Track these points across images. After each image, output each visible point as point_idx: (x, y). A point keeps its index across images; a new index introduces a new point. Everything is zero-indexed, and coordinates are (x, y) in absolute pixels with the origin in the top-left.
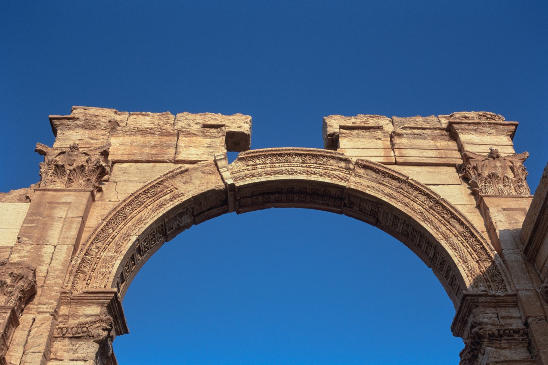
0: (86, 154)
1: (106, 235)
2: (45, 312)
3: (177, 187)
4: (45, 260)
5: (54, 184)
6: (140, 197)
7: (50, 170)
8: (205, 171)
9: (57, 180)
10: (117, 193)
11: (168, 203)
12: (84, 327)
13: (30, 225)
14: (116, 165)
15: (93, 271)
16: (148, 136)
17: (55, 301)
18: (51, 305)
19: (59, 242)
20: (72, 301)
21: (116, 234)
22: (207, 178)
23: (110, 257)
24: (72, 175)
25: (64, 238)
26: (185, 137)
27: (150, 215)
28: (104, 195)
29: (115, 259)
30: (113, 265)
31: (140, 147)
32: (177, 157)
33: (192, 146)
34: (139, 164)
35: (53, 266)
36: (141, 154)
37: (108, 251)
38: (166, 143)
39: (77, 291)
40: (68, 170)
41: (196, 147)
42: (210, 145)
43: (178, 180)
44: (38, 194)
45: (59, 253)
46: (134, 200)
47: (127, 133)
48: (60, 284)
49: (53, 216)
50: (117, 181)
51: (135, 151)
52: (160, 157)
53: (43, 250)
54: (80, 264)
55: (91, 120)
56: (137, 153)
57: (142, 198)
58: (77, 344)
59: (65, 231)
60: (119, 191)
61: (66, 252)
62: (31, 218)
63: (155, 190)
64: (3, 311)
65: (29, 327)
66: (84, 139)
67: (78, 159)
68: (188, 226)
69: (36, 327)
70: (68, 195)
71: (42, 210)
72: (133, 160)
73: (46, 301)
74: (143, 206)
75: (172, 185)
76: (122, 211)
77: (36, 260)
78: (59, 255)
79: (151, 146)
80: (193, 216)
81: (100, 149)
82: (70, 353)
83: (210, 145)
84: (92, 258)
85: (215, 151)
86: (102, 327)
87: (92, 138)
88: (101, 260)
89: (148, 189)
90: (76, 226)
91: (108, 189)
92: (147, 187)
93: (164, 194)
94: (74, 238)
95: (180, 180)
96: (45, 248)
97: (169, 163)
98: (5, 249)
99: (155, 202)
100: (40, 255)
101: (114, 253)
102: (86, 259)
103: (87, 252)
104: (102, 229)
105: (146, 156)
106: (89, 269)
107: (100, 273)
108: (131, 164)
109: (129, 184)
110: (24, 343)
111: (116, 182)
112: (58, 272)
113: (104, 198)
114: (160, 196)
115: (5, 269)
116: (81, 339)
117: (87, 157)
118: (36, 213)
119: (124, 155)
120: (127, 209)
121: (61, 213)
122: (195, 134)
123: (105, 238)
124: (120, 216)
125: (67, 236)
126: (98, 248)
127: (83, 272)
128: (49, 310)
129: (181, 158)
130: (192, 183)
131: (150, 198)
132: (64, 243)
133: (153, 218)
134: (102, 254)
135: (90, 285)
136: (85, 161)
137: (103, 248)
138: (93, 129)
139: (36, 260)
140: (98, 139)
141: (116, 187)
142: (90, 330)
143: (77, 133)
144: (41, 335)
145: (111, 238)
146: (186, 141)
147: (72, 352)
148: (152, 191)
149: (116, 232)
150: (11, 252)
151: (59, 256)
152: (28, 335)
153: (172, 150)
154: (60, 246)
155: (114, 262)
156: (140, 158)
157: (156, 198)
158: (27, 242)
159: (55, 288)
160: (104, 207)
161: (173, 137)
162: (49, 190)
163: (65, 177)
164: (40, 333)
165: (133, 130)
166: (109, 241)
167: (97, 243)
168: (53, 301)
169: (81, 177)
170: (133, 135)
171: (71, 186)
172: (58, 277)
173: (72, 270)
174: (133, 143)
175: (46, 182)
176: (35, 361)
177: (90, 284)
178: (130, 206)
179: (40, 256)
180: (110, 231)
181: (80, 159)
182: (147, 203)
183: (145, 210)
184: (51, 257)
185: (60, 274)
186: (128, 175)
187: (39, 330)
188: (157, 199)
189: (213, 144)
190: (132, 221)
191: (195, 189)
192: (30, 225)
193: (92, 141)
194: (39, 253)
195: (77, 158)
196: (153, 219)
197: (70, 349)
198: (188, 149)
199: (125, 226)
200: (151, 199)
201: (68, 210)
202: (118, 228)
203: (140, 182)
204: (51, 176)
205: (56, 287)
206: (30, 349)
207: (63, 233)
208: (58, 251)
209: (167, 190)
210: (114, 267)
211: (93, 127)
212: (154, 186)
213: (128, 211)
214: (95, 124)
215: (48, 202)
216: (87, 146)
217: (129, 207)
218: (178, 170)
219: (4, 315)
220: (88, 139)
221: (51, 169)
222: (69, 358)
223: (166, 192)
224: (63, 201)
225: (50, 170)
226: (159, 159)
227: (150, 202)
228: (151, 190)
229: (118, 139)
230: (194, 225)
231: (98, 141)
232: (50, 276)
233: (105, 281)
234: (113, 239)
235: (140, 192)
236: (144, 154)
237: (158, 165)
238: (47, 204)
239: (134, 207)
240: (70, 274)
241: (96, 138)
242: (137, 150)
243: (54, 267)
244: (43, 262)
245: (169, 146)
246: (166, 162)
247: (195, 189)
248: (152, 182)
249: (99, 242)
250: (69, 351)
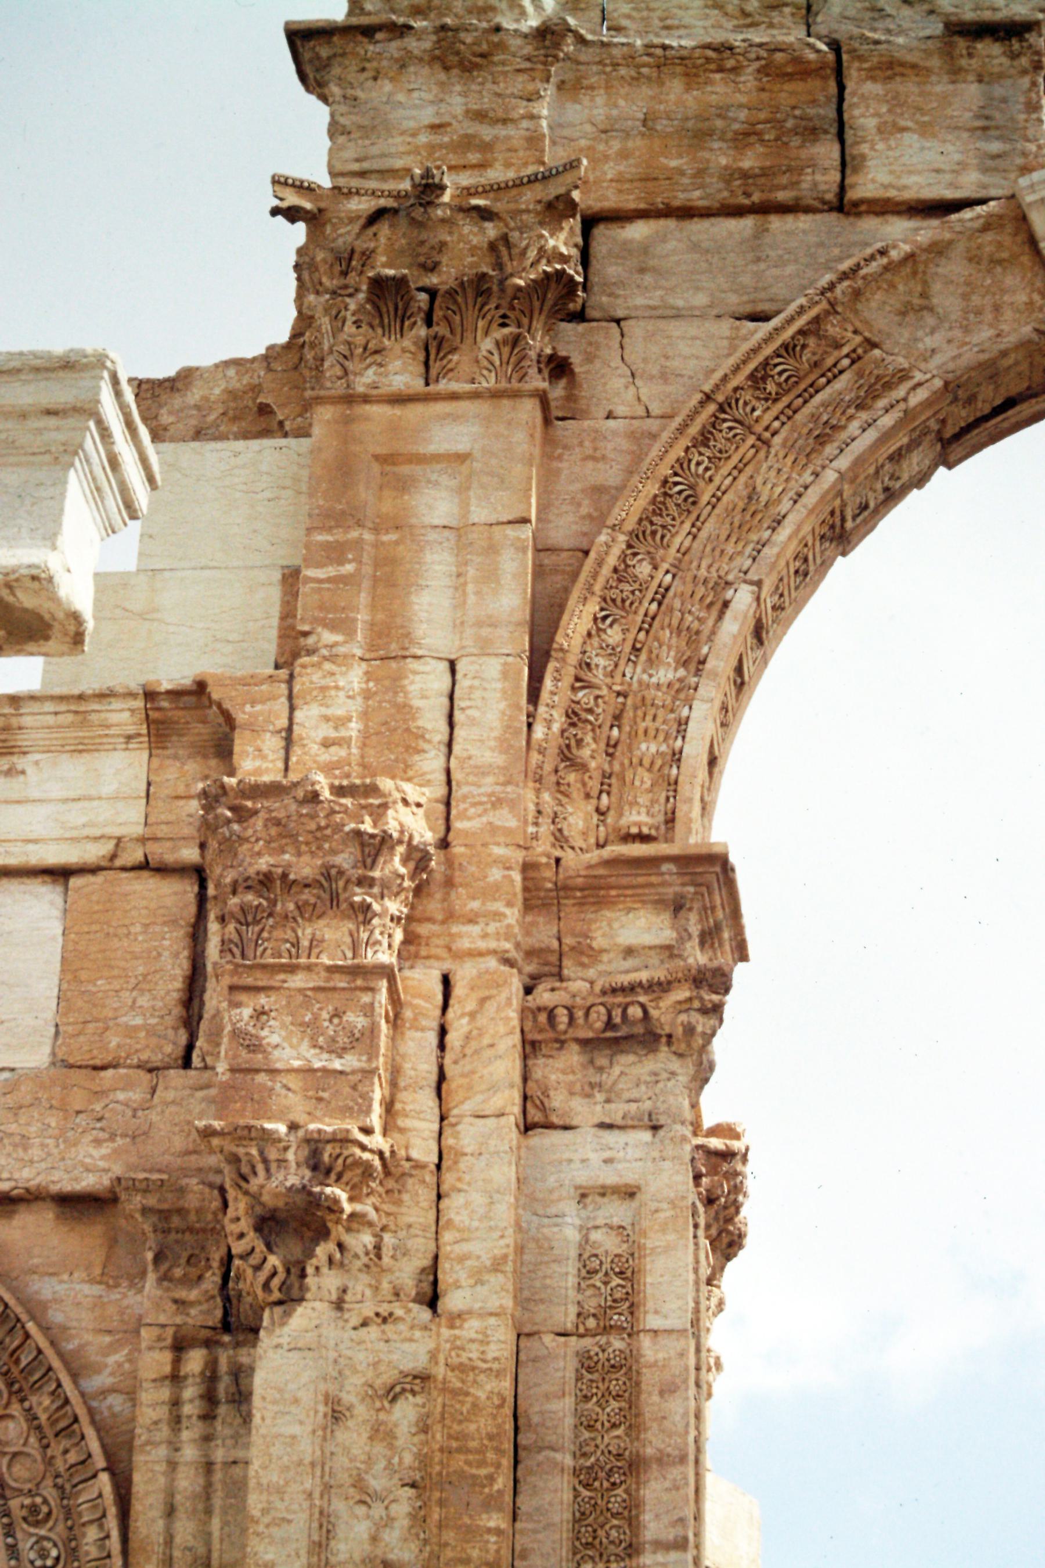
0: (485, 214)
1: (633, 592)
2: (481, 954)
3: (876, 339)
4: (429, 726)
5: (380, 365)
6: (737, 401)
7: (350, 295)
8: (979, 253)
9: (386, 342)
10: (633, 375)
11: (851, 418)
12: (632, 1003)
13: (331, 571)
14: (600, 232)
15: (611, 750)
16: (711, 82)
17: (510, 904)
18: (498, 924)
19: (465, 643)
20: (562, 893)
21: (669, 577)
22: (989, 281)
23: (664, 689)
24: (446, 318)
25: (479, 624)
26: (873, 79)
27: (787, 480)
28: (581, 386)
29: (682, 696)
31: (686, 141)
32: (852, 186)
33: (910, 124)
34: (698, 227)
35: (465, 754)
36: (700, 173)
37: (650, 660)
38: (797, 112)
39: (573, 848)
40: (420, 289)
41: (925, 130)
42: (987, 118)
43: (873, 304)
44: (328, 416)
45: (477, 694)
46: (715, 422)
47: (623, 71)
48: (508, 832)
49: (414, 521)
50: (620, 314)
51: (674, 163)
52: (785, 188)
53: (412, 682)
54: (563, 731)
55: (467, 30)
56: (682, 173)
57: (746, 404)
58: (611, 1063)
59: (478, 593)
60: (639, 366)
61: (504, 691)
62: (330, 538)
63: (791, 361)
64: (359, 982)
65: (438, 1012)
66: (449, 124)
67: (455, 238)
68: (920, 480)
69: (463, 1015)
70: (449, 415)
71: (363, 495)
72: (667, 205)
73: (475, 905)
74: (751, 440)
75: (855, 332)
76: (676, 474)
77: (395, 730)
78: (479, 703)
79: (736, 133)
80: (941, 440)
81: (538, 186)
82: (592, 1101)
83: (987, 118)
84: (597, 697)
85: (1008, 147)
86: (696, 1004)
87: (480, 116)
88: (630, 701)
89: (765, 364)
90: (515, 564)
91: (590, 359)
92: (760, 358)
93: (829, 374)
94: (519, 624)
95: (884, 303)
96: (415, 673)
97: (822, 211)
98: (264, 687)
99: (798, 417)
100: (405, 705)
101: (676, 670)
102: (577, 708)
103: (578, 679)
104: (615, 570)
105: (721, 185)
106: (594, 746)
107: (641, 764)
108: (662, 222)
109: (675, 328)
110: (434, 1077)
111: (618, 321)
112: (490, 779)
113: (583, 403)
114: (811, 385)
115: (327, 816)
116: (624, 1045)
117: (491, 230)
118: (343, 512)
119: (627, 186)
120: (694, 462)
122: (914, 66)
123: (632, 604)
124: (671, 496)
125: (490, 617)
126: (612, 652)
127: (583, 767)
128: (493, 944)
129: (871, 186)
130: (931, 309)
131: (775, 401)
132: (485, 649)
133: (800, 495)
134: (628, 675)
135: (612, 813)
136: (485, 245)
137: (628, 648)
138: (476, 66)
139: (395, 730)
140: (512, 120)
141: (622, 348)
142: (654, 1013)
143: (416, 94)
144: (492, 1046)
145: (653, 600)
146: (877, 98)
147: (600, 1097)
148: (779, 368)
149: (667, 572)
150: (290, 697)
151: (477, 707)
152: (442, 1046)
153: (827, 151)
154: (472, 663)
155: (685, 712)
156: (696, 197)
157: (799, 396)
158: (342, 650)
159: (498, 851)
160: (595, 449)
161: (818, 83)
162: (366, 399)
163: (415, 323)
164: (486, 1041)
165: (646, 59)
166: (646, 615)
167: (604, 631)
168: (499, 906)
169: (481, 324)
170: (649, 79)
171: (451, 370)
172: (497, 802)
173: (540, 767)
174: (654, 120)
175: (345, 357)
176: (492, 1149)
177: (608, 809)
178: (702, 449)
179: (405, 710)
180: (644, 569)
181: (462, 238)
182: (765, 423)
183: (762, 454)
184: (445, 710)
185: (498, 788)
186: (663, 283)
187: (479, 1024)
188: (800, 400)
189: (997, 115)
190: (716, 511)
191: (949, 341)
192: (331, 571)
193: (487, 132)
194: (400, 699)
195: (450, 233)
196: (804, 500)
197: (590, 1083)
198: (892, 143)
199: (695, 537)
200: (780, 405)
202: (673, 551)
203: (719, 317)
204: (357, 324)
205: (498, 844)
206: (462, 1102)
207: (472, 599)
208: (471, 687)
209: (836, 354)
210: (688, 735)
211: (478, 60)
212: (785, 346)
213: (701, 469)
214: (485, 47)
215: (377, 457)
216: (473, 157)
217: (701, 454)
218: (874, 264)
219: (366, 998)
220: (466, 123)
221: (351, 290)
222: (596, 1121)
223: (835, 365)
224: (432, 448)
225: (348, 300)
226: (782, 196)
227: (777, 418)
228: (776, 365)
229: (586, 100)
230: (942, 470)
231: (510, 131)
232: (465, 797)
233: (664, 795)
234: (660, 604)
235: (734, 383)
236: (712, 176)
237: (776, 223)
238: (376, 468)
239: (720, 452)
240: (537, 785)
241: (500, 114)
242: (680, 156)
243: (470, 758)
244: (423, 737)
245: (811, 132)
246: (808, 210)
247: (949, 341)
248: (776, 329)
249: (611, 625)
250: (587, 1088)
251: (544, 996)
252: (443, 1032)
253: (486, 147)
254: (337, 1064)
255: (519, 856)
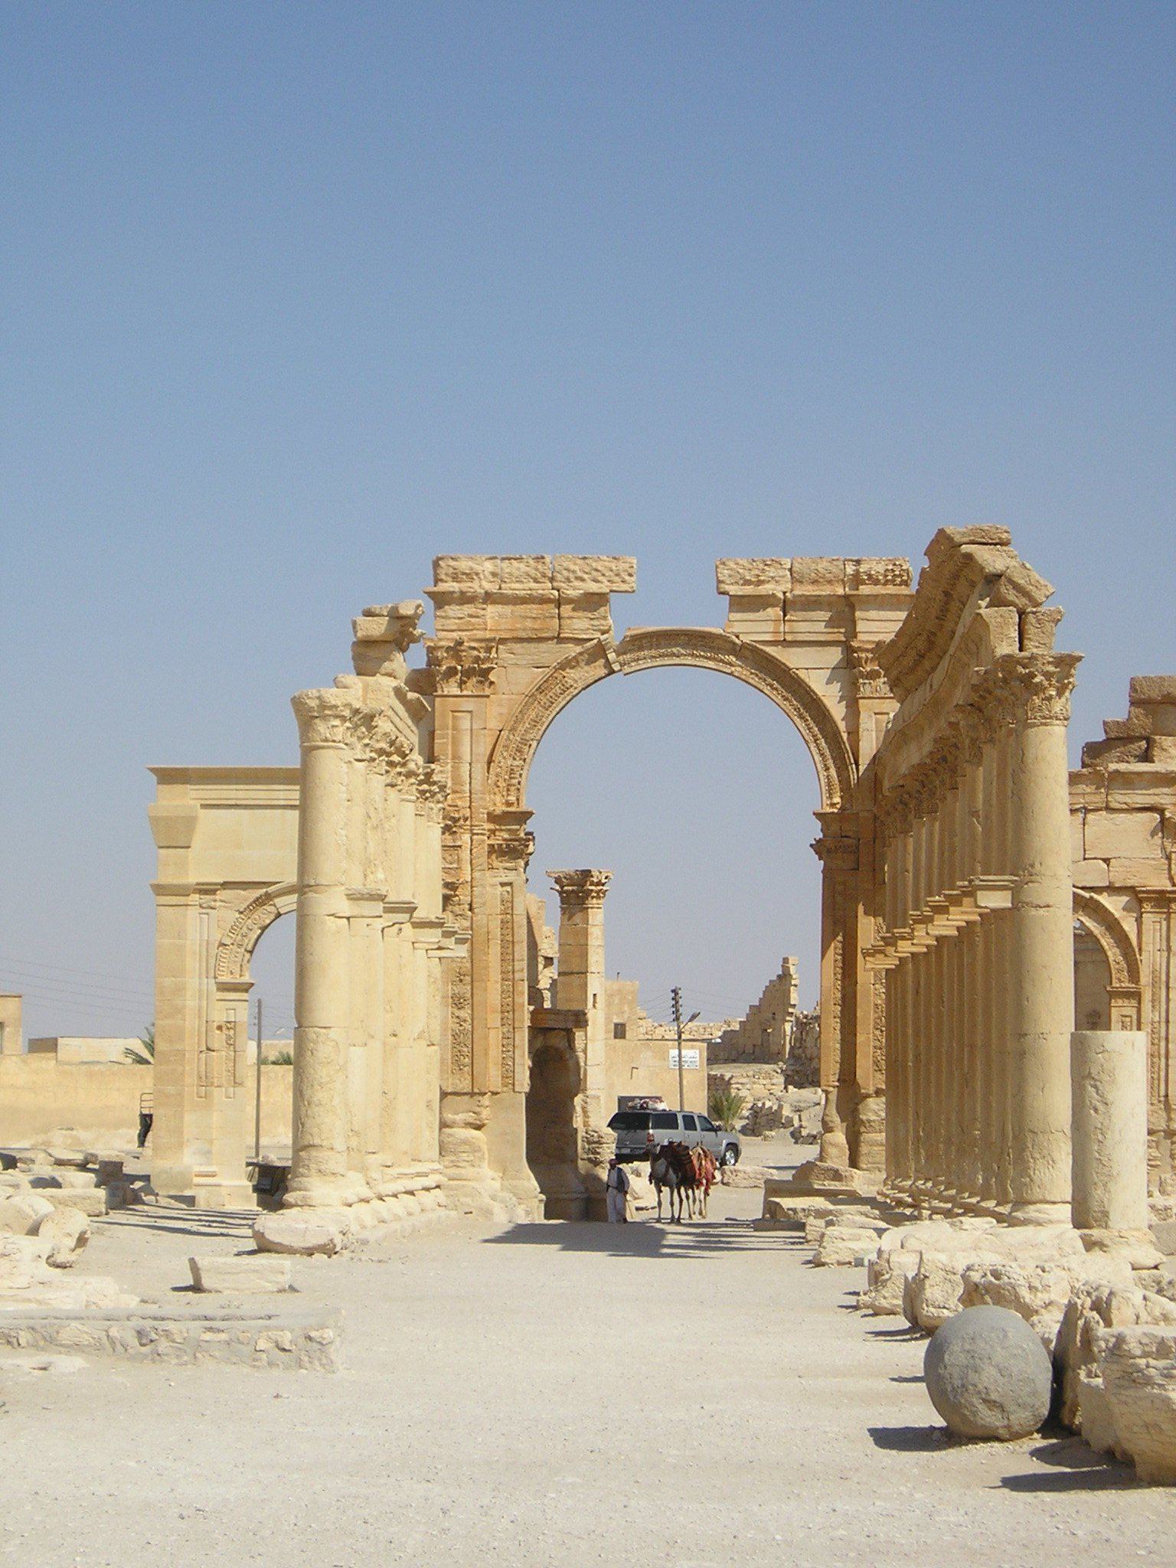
0: (474, 648)
30: (521, 775)
87: (470, 616)
117: (475, 653)
121: (465, 723)
152: (471, 854)
156: (524, 635)
180: (512, 737)
201: (471, 719)
216: (471, 628)
226: (544, 635)
251: (491, 842)
252: (471, 850)
253: (473, 624)
254: (451, 866)
255: (486, 811)
